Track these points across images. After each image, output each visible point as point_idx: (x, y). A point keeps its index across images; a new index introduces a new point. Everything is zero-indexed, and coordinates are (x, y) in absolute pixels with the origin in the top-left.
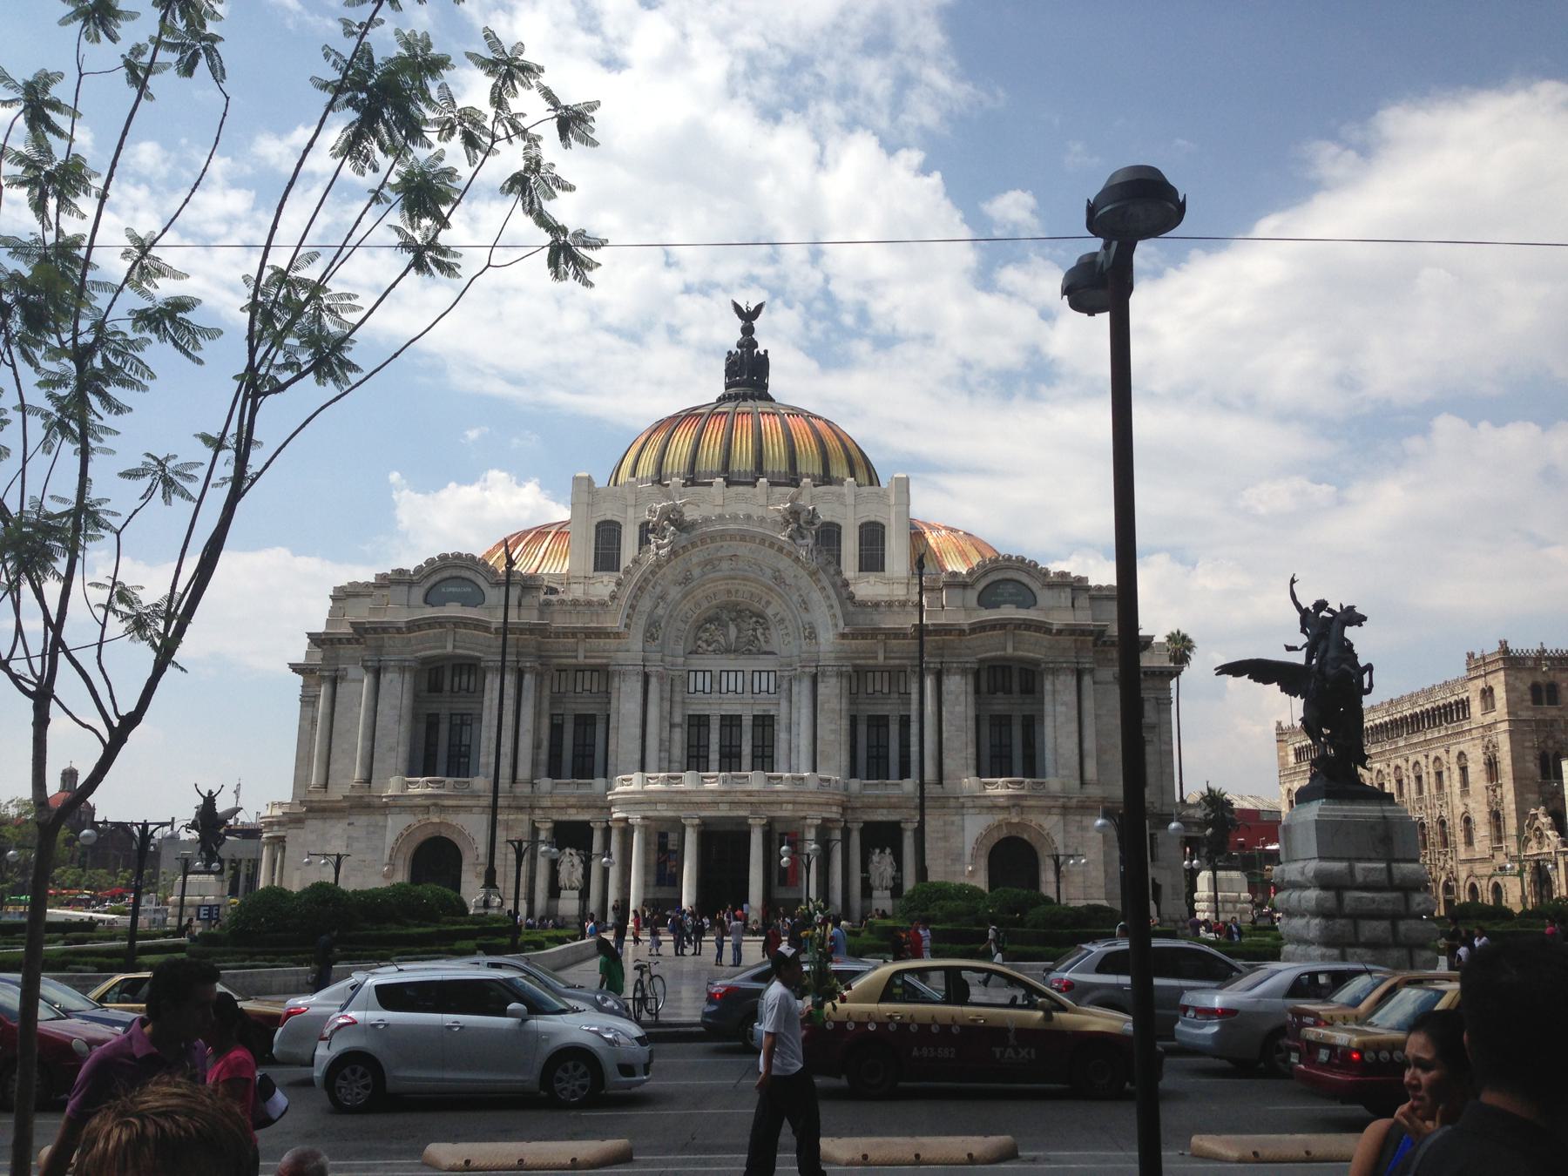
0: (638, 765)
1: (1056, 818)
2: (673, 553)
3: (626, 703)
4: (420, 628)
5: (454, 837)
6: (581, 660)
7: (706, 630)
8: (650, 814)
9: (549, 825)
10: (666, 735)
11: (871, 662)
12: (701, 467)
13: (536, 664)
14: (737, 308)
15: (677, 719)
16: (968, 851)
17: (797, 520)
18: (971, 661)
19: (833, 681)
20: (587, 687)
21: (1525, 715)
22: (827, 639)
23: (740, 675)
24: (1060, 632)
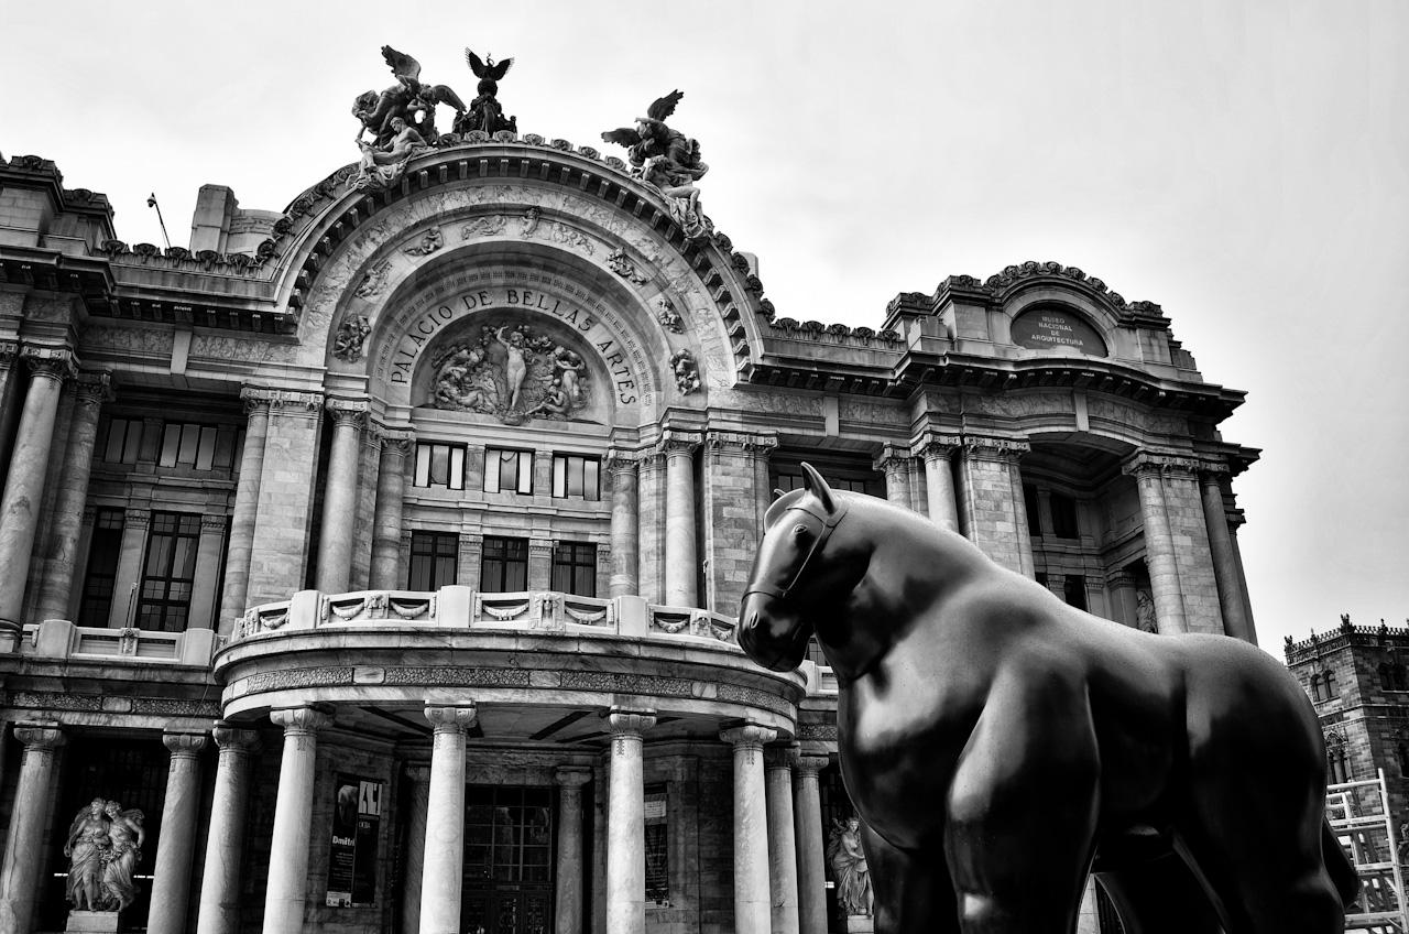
0: (298, 578)
3: (277, 472)
6: (178, 365)
7: (459, 362)
8: (334, 695)
9: (50, 734)
10: (363, 559)
11: (812, 433)
13: (65, 355)
14: (474, 61)
15: (391, 529)
18: (1019, 437)
19: (739, 463)
20: (187, 456)
21: (1379, 702)
22: (723, 375)
23: (525, 460)
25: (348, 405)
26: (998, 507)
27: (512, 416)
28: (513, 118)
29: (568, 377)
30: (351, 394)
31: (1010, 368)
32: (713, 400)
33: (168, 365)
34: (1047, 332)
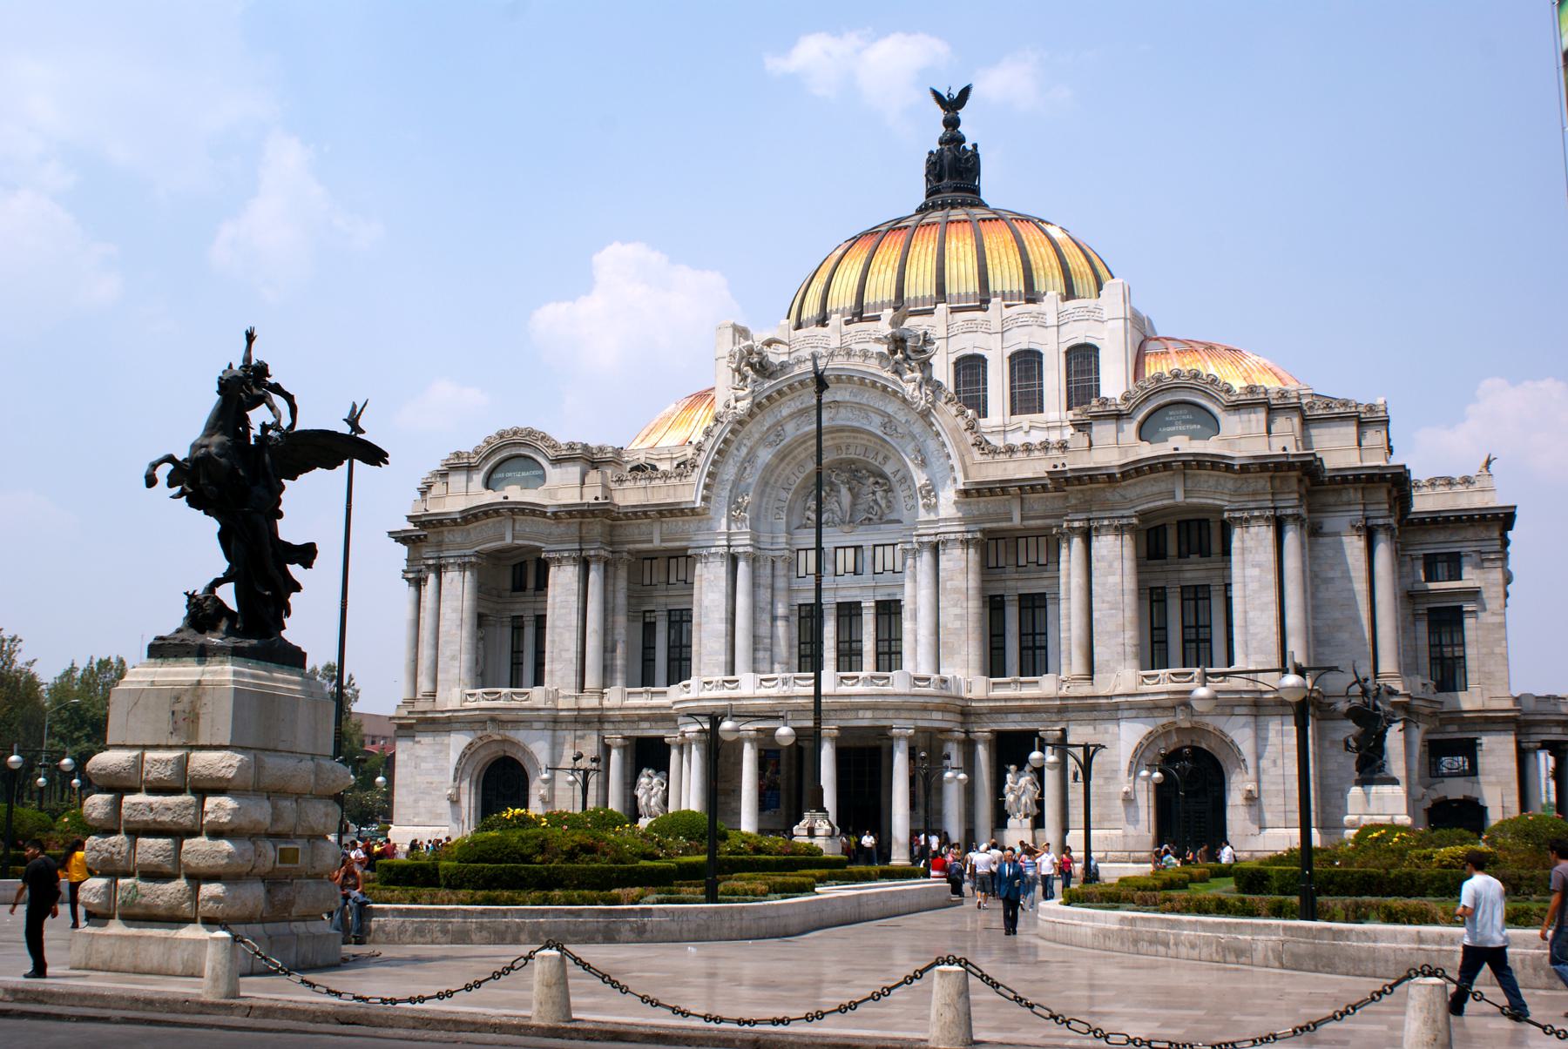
1: (1243, 720)
2: (758, 406)
4: (476, 517)
5: (519, 756)
6: (657, 543)
11: (1004, 525)
12: (869, 298)
13: (602, 553)
14: (938, 97)
15: (781, 610)
16: (1124, 765)
17: (904, 350)
18: (1129, 515)
24: (1244, 469)
25: (741, 550)
26: (1110, 566)
27: (846, 528)
28: (975, 146)
29: (879, 494)
30: (743, 543)
31: (1115, 471)
32: (943, 513)
33: (651, 541)
34: (1171, 424)
